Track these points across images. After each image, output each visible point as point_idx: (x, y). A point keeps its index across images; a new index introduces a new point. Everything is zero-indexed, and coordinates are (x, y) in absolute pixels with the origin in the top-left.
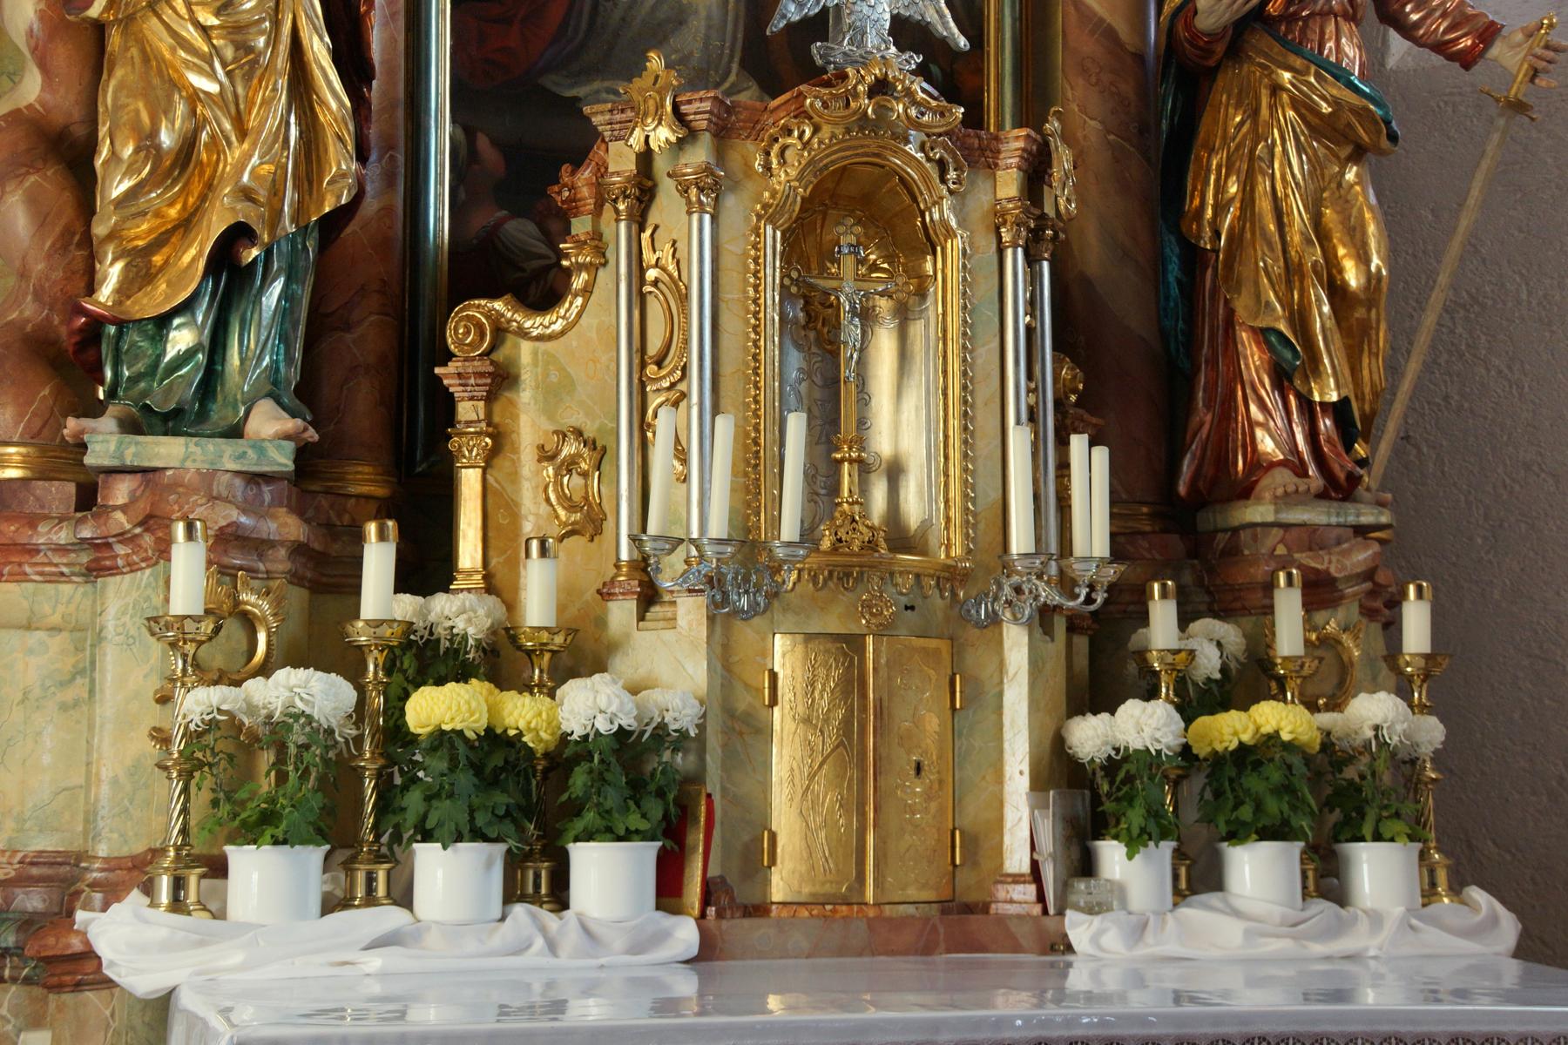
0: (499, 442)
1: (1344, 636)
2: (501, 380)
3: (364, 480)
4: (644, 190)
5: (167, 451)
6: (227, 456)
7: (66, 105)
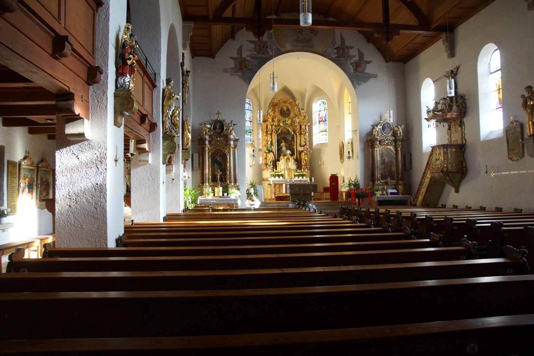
0: (278, 166)
1: (293, 171)
2: (278, 164)
3: (275, 167)
4: (282, 159)
5: (269, 167)
6: (271, 167)
7: (266, 157)
